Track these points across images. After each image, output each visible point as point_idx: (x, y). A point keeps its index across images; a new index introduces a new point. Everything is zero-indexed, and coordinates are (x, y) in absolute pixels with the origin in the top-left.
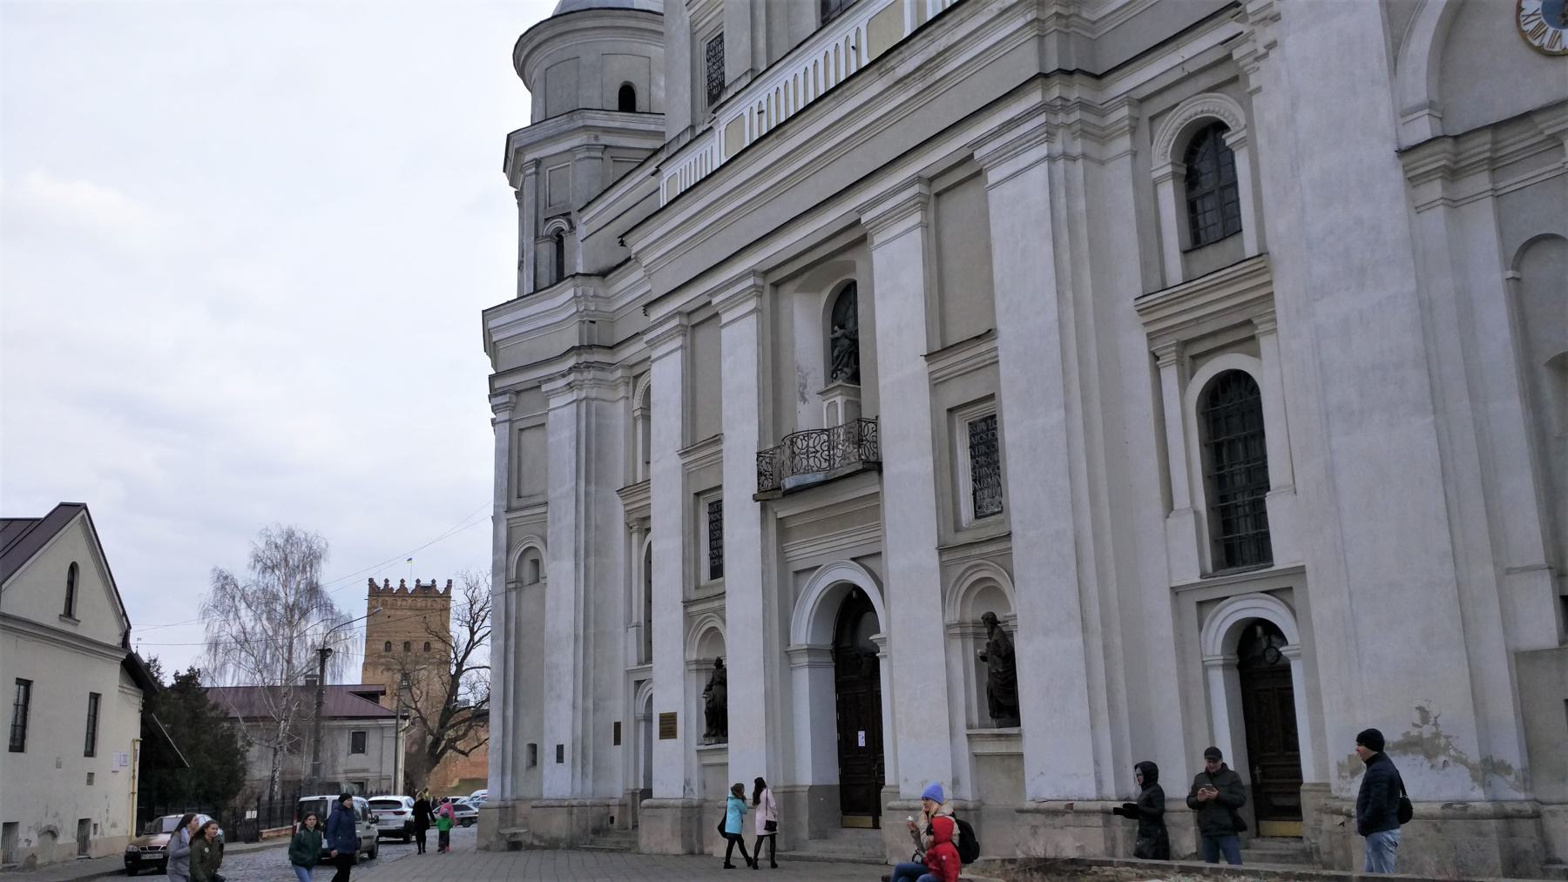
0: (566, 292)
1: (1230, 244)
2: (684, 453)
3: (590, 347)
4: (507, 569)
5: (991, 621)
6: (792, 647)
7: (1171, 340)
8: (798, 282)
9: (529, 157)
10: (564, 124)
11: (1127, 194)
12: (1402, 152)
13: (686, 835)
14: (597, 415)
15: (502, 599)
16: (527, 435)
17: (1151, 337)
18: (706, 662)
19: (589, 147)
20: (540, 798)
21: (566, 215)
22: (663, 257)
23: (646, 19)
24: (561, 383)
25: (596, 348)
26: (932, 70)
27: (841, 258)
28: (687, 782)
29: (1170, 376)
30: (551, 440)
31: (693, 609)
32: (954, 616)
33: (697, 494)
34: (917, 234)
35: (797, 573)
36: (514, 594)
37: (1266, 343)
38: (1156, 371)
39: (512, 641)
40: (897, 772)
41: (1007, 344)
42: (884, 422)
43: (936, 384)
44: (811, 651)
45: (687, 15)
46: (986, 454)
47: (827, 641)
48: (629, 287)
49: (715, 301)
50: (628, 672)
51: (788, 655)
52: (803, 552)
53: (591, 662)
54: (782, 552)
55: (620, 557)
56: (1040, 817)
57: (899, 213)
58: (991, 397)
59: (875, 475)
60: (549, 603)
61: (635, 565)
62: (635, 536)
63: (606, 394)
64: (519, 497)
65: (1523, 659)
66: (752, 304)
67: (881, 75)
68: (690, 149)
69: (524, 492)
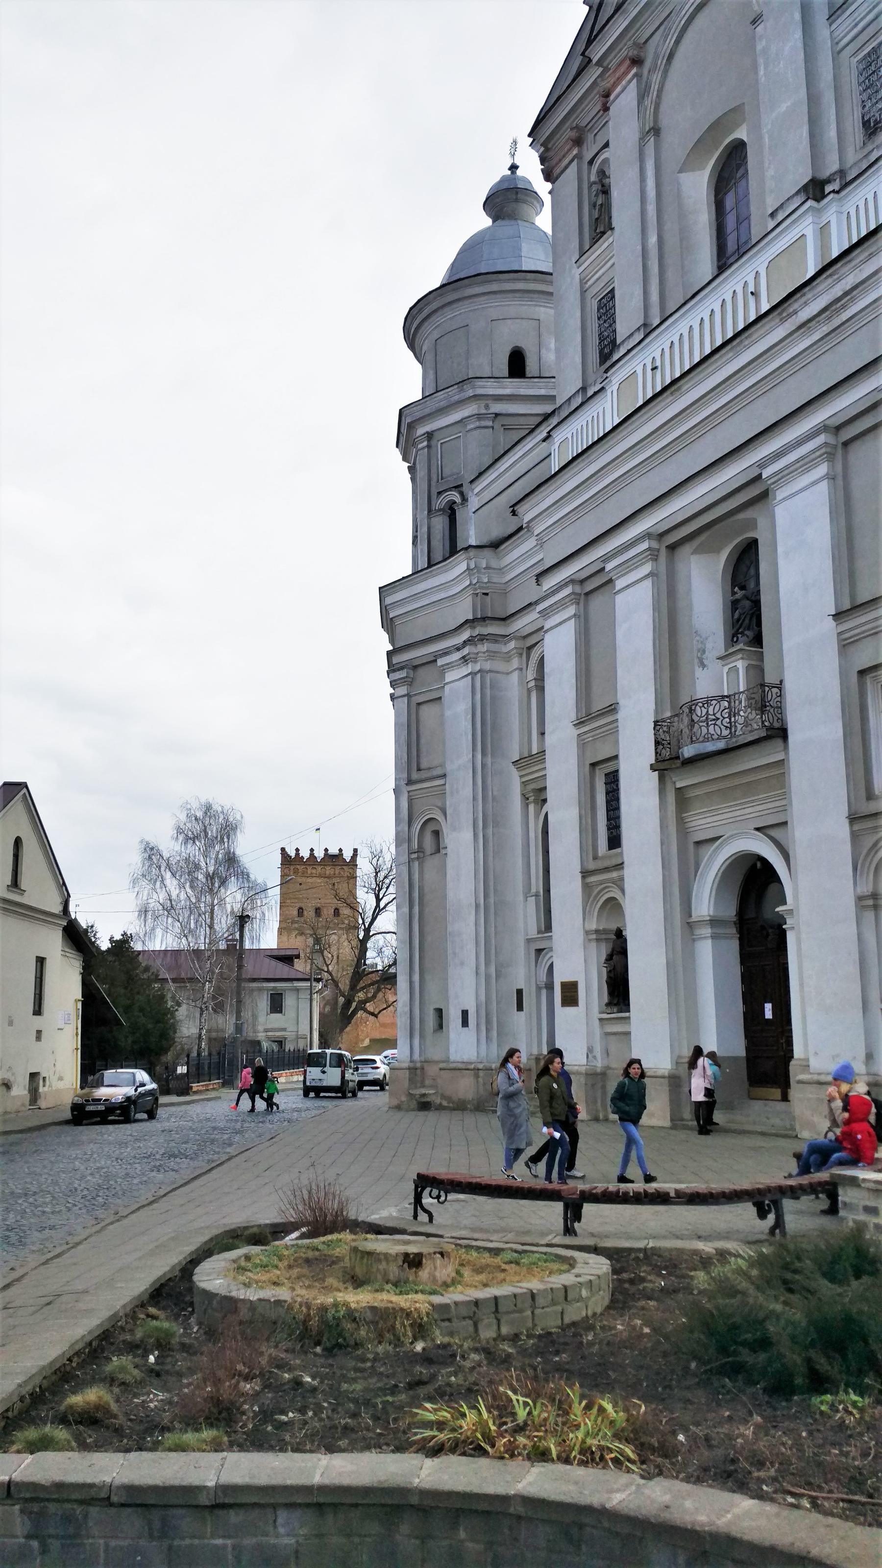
0: (460, 565)
2: (579, 724)
3: (484, 619)
4: (409, 840)
6: (694, 918)
9: (421, 431)
10: (455, 394)
14: (492, 687)
15: (405, 869)
18: (605, 931)
19: (479, 417)
20: (447, 1061)
21: (458, 487)
22: (556, 526)
23: (535, 280)
24: (456, 656)
25: (489, 619)
26: (838, 311)
27: (741, 516)
28: (590, 1050)
30: (448, 713)
31: (592, 879)
33: (593, 765)
34: (824, 486)
35: (698, 843)
36: (416, 864)
39: (416, 909)
40: (806, 1045)
42: (788, 686)
43: (845, 645)
44: (714, 922)
47: (730, 911)
48: (521, 557)
49: (609, 566)
50: (529, 941)
51: (690, 926)
52: (703, 823)
53: (492, 930)
54: (681, 822)
55: (518, 829)
57: (805, 464)
59: (779, 742)
60: (450, 873)
61: (532, 835)
62: (531, 808)
63: (500, 666)
64: (419, 770)
66: (647, 568)
67: (783, 320)
68: (580, 413)
69: (424, 765)
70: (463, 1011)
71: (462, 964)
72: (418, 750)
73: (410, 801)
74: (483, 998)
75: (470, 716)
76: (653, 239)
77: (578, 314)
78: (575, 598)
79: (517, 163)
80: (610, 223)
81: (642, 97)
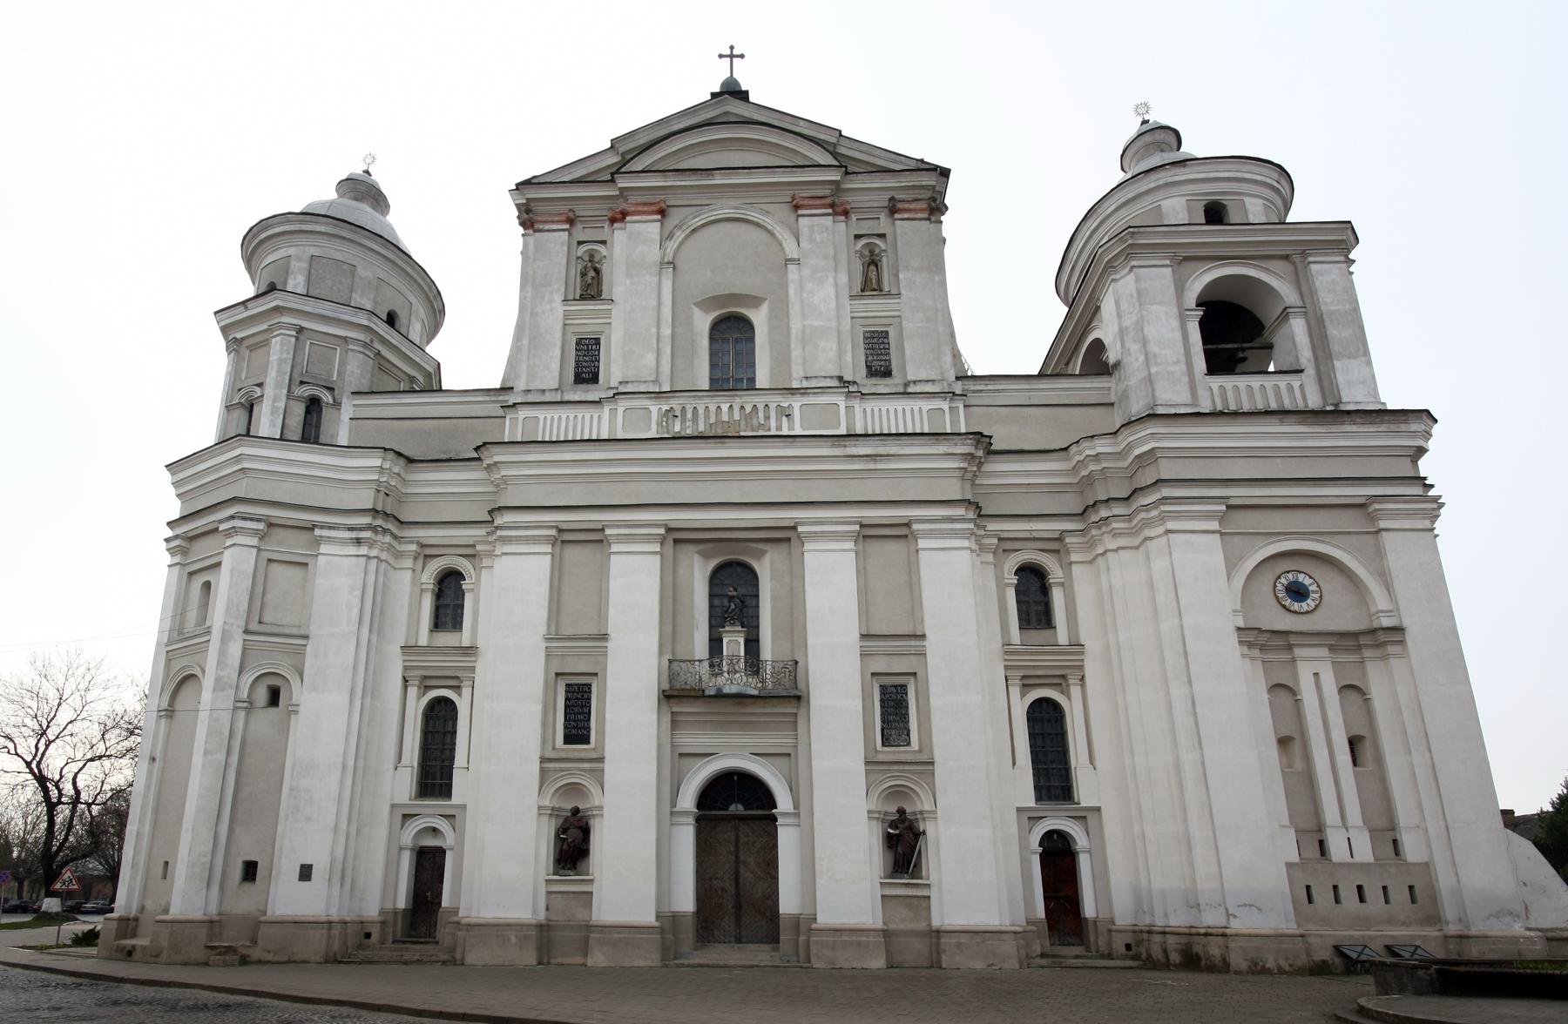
4: (237, 687)
6: (678, 808)
8: (701, 547)
9: (286, 319)
11: (992, 585)
13: (540, 949)
15: (225, 718)
16: (278, 571)
17: (1007, 668)
18: (560, 809)
28: (534, 905)
29: (1015, 691)
30: (319, 581)
31: (552, 765)
33: (557, 674)
36: (242, 715)
39: (235, 758)
41: (932, 645)
45: (560, 309)
51: (672, 813)
52: (693, 740)
59: (794, 702)
67: (833, 446)
69: (265, 619)
70: (303, 867)
71: (308, 819)
72: (262, 604)
73: (244, 650)
74: (340, 854)
75: (358, 593)
76: (667, 331)
77: (558, 335)
78: (554, 541)
80: (600, 293)
81: (666, 237)
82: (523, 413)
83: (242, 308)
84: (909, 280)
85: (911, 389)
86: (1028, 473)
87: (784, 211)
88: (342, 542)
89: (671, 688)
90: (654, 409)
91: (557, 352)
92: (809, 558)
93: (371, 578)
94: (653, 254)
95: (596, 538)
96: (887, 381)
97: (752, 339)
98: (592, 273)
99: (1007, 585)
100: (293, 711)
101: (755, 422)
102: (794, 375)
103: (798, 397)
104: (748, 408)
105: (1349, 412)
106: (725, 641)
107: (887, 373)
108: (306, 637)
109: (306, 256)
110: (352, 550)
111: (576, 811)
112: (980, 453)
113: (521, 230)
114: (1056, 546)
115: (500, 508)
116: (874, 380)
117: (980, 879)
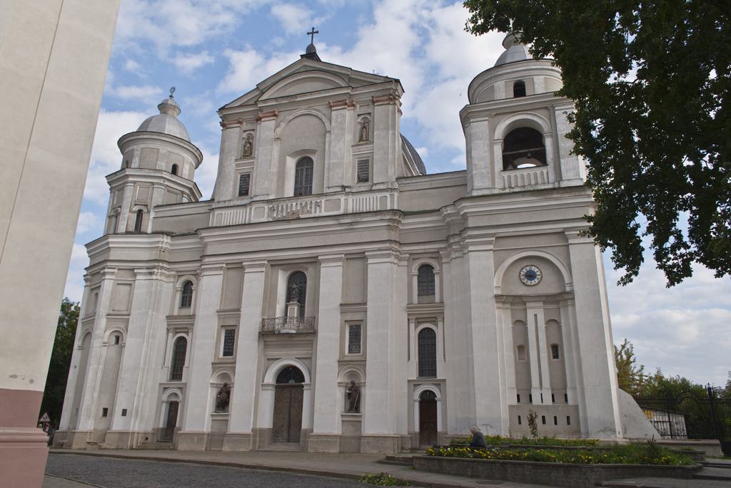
1: (431, 297)
5: (353, 383)
6: (265, 382)
7: (414, 317)
9: (130, 179)
12: (497, 297)
17: (408, 315)
29: (412, 326)
32: (339, 380)
33: (222, 326)
35: (268, 359)
37: (440, 324)
38: (409, 323)
46: (356, 335)
52: (273, 353)
56: (370, 440)
58: (362, 320)
62: (170, 334)
65: (511, 407)
67: (334, 220)
77: (232, 175)
79: (173, 95)
80: (251, 154)
81: (277, 126)
82: (217, 212)
83: (114, 175)
84: (377, 134)
85: (374, 188)
86: (424, 223)
87: (324, 109)
88: (145, 274)
89: (262, 331)
90: (266, 207)
91: (232, 183)
92: (323, 270)
93: (154, 289)
94: (271, 135)
95: (240, 267)
96: (366, 184)
97: (312, 168)
98: (248, 145)
99: (413, 275)
100: (122, 347)
101: (305, 210)
102: (325, 186)
103: (324, 197)
104: (303, 204)
105: (564, 188)
106: (289, 308)
107: (366, 180)
108: (129, 315)
109: (139, 149)
110: (149, 277)
111: (225, 385)
112: (397, 217)
113: (222, 128)
114: (436, 255)
115: (203, 256)
116: (360, 184)
117: (388, 414)
